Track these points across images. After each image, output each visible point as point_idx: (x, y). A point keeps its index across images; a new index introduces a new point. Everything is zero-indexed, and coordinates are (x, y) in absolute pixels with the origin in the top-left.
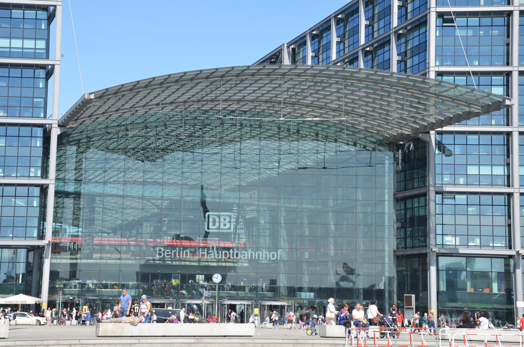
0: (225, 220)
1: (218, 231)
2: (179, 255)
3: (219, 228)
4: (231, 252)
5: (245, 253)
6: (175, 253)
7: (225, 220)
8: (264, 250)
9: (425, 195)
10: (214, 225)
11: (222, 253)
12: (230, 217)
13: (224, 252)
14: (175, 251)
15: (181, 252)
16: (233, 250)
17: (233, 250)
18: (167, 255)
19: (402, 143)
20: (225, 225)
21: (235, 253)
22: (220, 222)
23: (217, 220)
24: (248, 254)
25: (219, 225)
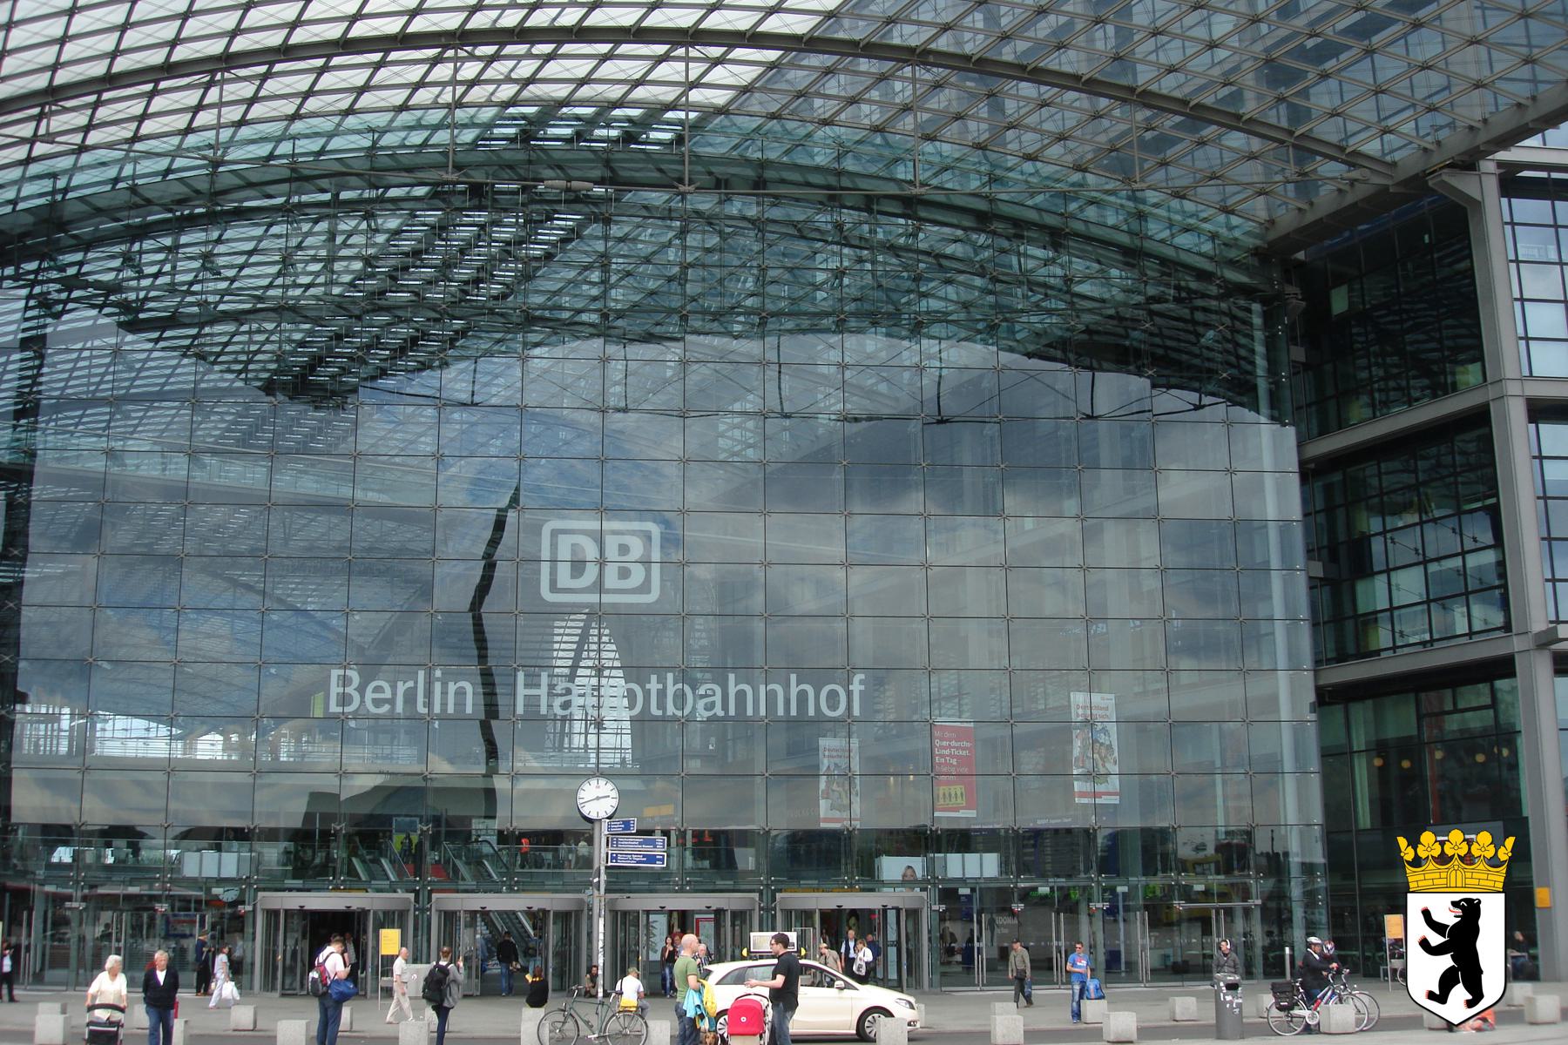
0: (624, 549)
2: (429, 704)
3: (599, 586)
4: (654, 686)
6: (410, 697)
7: (624, 549)
9: (1480, 419)
12: (647, 537)
15: (438, 687)
16: (662, 680)
17: (662, 680)
18: (378, 703)
19: (1301, 255)
20: (624, 574)
21: (671, 690)
22: (602, 562)
23: (591, 552)
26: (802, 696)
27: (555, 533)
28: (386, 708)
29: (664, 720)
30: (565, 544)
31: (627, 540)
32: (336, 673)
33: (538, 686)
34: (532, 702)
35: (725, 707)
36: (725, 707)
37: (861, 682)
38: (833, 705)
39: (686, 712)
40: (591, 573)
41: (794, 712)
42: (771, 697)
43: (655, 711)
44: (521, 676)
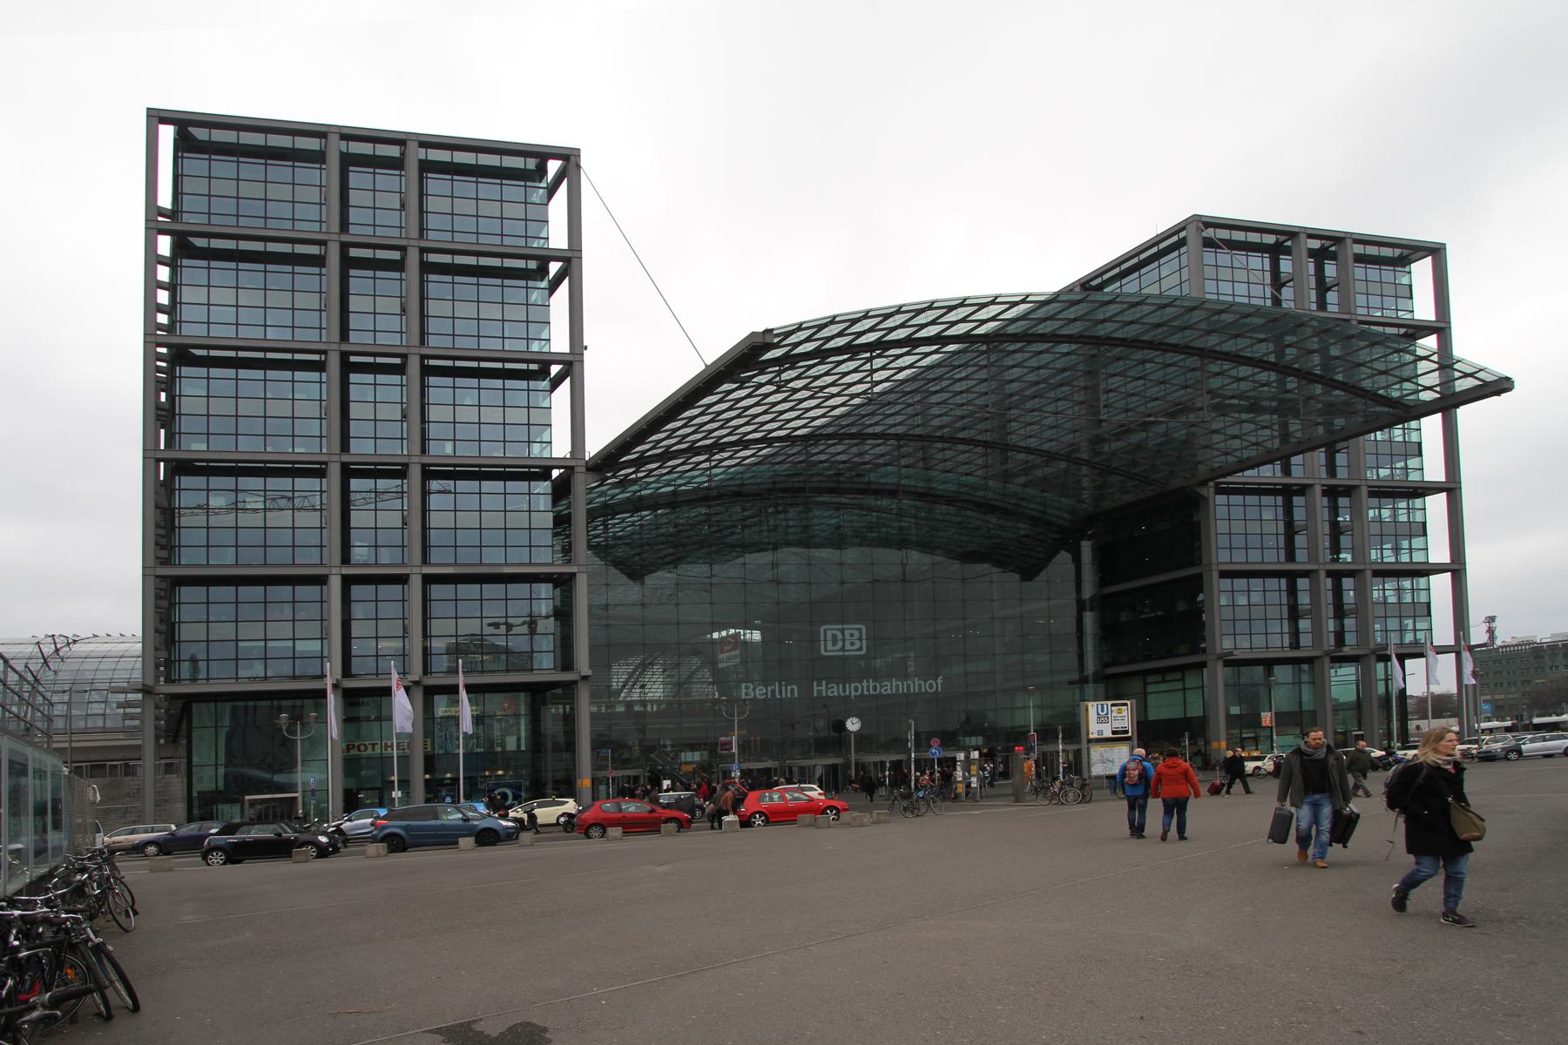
0: (852, 635)
2: (780, 693)
3: (843, 649)
4: (865, 684)
5: (886, 686)
6: (773, 692)
7: (852, 635)
10: (834, 644)
11: (850, 686)
12: (860, 630)
13: (853, 685)
14: (773, 687)
15: (784, 687)
16: (868, 682)
17: (868, 682)
20: (852, 644)
24: (892, 686)
25: (844, 646)
26: (920, 685)
27: (825, 631)
29: (869, 695)
30: (829, 634)
31: (854, 632)
32: (743, 685)
33: (821, 685)
34: (820, 692)
38: (931, 688)
39: (878, 691)
40: (840, 644)
41: (917, 691)
42: (908, 686)
43: (866, 693)
44: (815, 683)
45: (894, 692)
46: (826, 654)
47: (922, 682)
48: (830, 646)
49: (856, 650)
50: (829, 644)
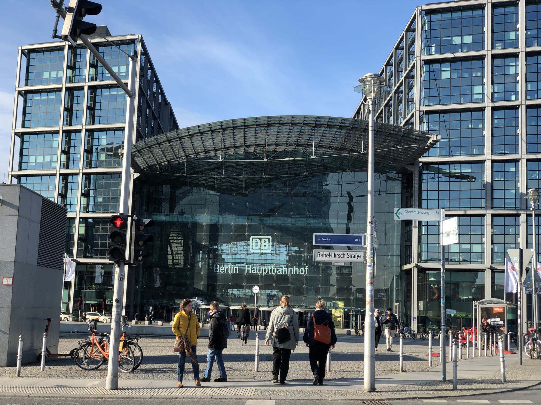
0: (265, 241)
1: (259, 251)
2: (230, 271)
5: (279, 269)
6: (227, 269)
8: (295, 266)
10: (256, 246)
12: (269, 239)
18: (222, 271)
25: (261, 246)
26: (296, 270)
27: (253, 238)
28: (223, 272)
34: (248, 271)
35: (282, 272)
36: (282, 272)
37: (308, 268)
38: (302, 272)
39: (275, 273)
40: (259, 246)
41: (295, 273)
42: (291, 270)
45: (283, 273)
46: (253, 251)
47: (298, 269)
48: (254, 247)
49: (267, 250)
50: (254, 245)
